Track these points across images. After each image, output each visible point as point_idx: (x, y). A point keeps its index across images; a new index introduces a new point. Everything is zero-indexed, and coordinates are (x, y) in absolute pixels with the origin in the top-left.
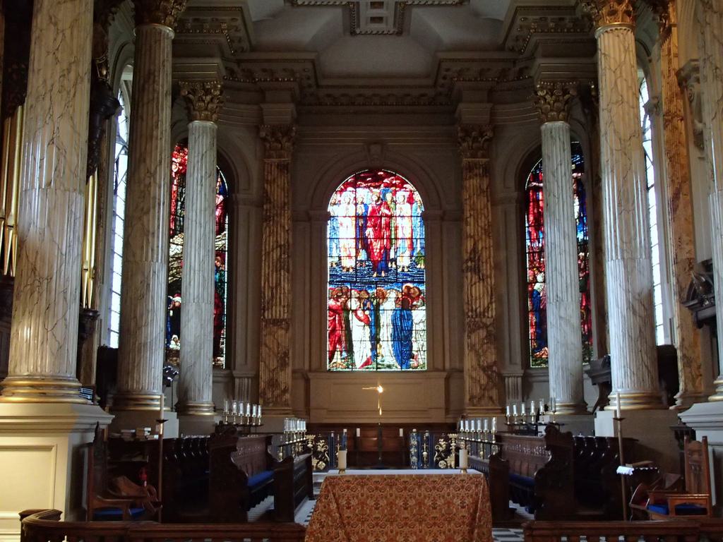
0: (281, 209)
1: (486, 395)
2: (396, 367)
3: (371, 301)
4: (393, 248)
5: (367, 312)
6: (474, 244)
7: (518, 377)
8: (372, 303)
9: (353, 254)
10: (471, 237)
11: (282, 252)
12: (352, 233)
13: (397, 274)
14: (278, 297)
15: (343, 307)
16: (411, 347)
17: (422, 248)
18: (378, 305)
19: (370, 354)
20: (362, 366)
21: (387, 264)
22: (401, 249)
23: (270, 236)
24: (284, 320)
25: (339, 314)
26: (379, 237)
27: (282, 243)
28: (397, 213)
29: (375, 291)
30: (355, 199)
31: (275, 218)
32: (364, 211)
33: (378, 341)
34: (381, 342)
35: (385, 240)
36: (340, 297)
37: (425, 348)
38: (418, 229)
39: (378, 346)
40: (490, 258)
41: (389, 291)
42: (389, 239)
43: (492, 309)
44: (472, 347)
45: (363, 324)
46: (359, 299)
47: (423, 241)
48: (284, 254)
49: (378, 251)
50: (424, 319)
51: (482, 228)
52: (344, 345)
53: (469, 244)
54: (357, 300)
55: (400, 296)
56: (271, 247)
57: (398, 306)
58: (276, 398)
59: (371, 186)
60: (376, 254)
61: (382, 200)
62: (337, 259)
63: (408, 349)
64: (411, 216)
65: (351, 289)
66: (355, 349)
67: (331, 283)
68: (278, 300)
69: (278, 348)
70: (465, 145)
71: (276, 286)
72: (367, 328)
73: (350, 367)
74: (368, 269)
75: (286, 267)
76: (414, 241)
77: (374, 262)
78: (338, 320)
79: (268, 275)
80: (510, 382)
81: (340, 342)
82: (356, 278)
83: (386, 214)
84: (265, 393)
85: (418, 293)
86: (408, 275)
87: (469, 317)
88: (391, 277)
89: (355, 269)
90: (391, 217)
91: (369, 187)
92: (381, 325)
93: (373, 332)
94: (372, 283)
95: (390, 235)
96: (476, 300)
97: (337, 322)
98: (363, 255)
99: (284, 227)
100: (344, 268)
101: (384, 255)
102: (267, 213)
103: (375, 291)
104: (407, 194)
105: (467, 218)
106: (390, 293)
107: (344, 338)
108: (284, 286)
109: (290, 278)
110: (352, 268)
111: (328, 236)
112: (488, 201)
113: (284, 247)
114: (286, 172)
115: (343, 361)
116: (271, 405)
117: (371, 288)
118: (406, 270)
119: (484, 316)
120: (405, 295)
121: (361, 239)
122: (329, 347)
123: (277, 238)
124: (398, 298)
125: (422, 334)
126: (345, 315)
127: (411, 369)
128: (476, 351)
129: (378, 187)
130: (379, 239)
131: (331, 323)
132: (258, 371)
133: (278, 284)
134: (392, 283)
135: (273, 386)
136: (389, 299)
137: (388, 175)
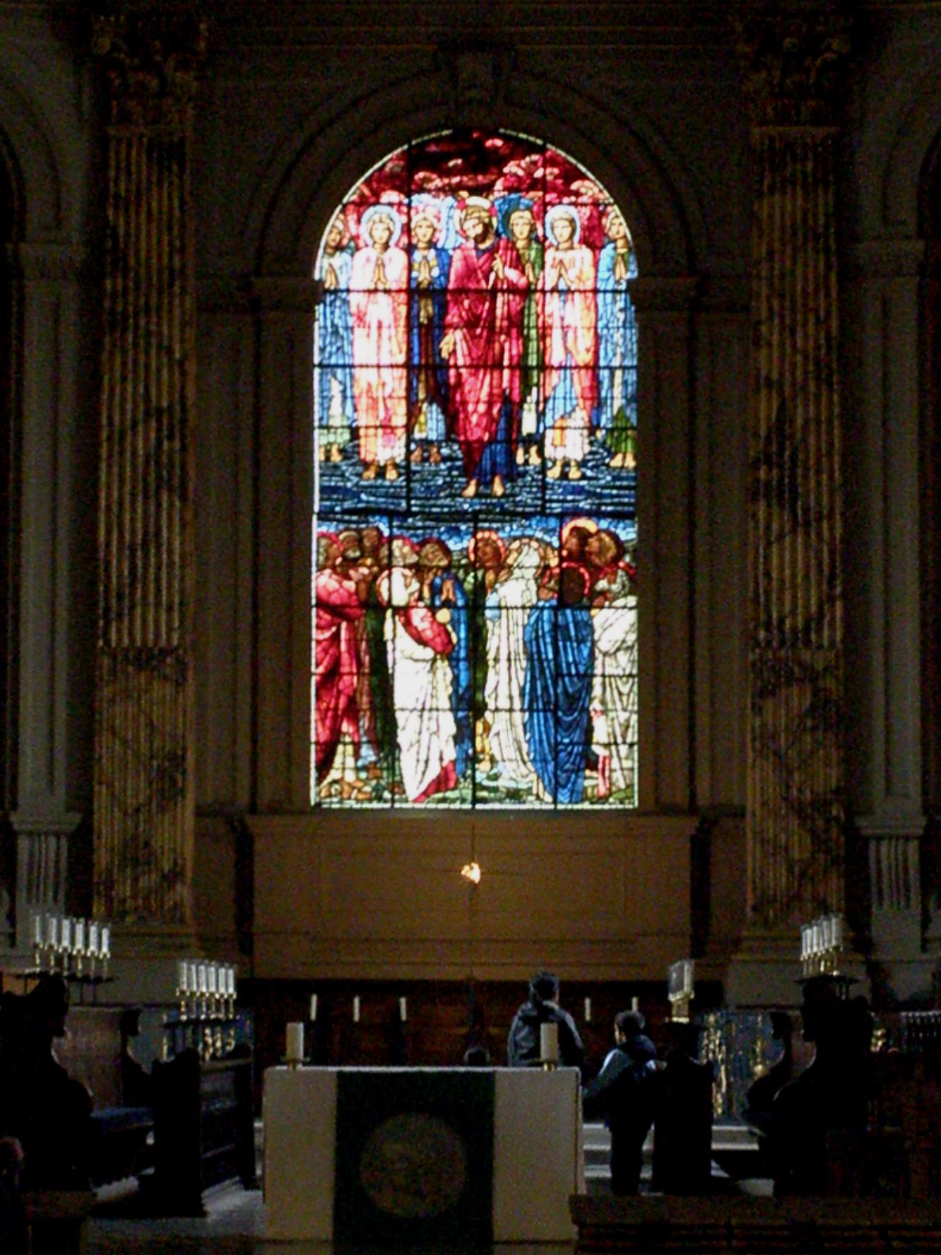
0: (160, 293)
1: (807, 894)
2: (538, 797)
3: (456, 578)
4: (532, 398)
5: (444, 615)
6: (782, 408)
7: (907, 838)
8: (459, 583)
9: (400, 419)
10: (769, 383)
11: (165, 433)
12: (394, 348)
13: (544, 487)
14: (152, 577)
15: (363, 595)
16: (589, 731)
17: (629, 400)
18: (481, 590)
19: (451, 753)
20: (426, 794)
21: (511, 455)
22: (559, 403)
23: (124, 379)
24: (165, 652)
25: (350, 620)
26: (486, 362)
27: (165, 404)
28: (550, 278)
29: (469, 543)
30: (407, 229)
31: (142, 322)
32: (436, 272)
33: (478, 709)
34: (488, 715)
35: (506, 373)
36: (354, 563)
37: (633, 736)
38: (618, 337)
39: (479, 727)
40: (830, 455)
41: (516, 545)
42: (522, 368)
43: (833, 619)
44: (766, 738)
45: (428, 653)
46: (418, 570)
47: (632, 377)
48: (171, 437)
49: (482, 408)
50: (632, 638)
51: (806, 357)
52: (365, 723)
53: (766, 408)
54: (407, 572)
55: (554, 562)
56: (129, 416)
57: (545, 594)
58: (146, 898)
59: (460, 186)
60: (474, 419)
61: (498, 235)
62: (347, 436)
63: (576, 736)
64: (595, 291)
65: (392, 538)
66: (403, 738)
67: (325, 516)
68: (152, 586)
69: (151, 743)
70: (759, 78)
71: (145, 543)
72: (443, 667)
73: (387, 795)
74: (450, 469)
75: (176, 482)
76: (604, 374)
77: (467, 446)
78: (348, 641)
79: (121, 504)
80: (885, 855)
81: (352, 712)
82: (408, 499)
83: (511, 284)
84: (110, 886)
85: (612, 552)
86: (579, 491)
87: (758, 644)
88: (524, 497)
89: (406, 470)
90: (526, 292)
91: (452, 191)
92: (491, 656)
93: (464, 681)
94: (461, 516)
95: (524, 355)
96: (781, 590)
97: (343, 646)
98: (432, 423)
99: (170, 351)
100: (366, 465)
101: (502, 424)
102: (114, 303)
103: (469, 543)
104: (581, 215)
105: (759, 323)
106: (519, 551)
107: (365, 699)
108: (170, 544)
109: (189, 516)
110: (396, 466)
111: (316, 360)
112: (828, 268)
113: (171, 417)
114: (175, 168)
115: (363, 775)
116: (129, 919)
117: (456, 532)
118: (574, 473)
119: (808, 643)
120: (570, 557)
121: (427, 366)
122: (317, 731)
123: (147, 387)
124: (547, 567)
125: (625, 690)
126: (370, 623)
127: (586, 806)
128: (776, 753)
129: (483, 190)
130: (485, 367)
131: (326, 651)
132: (88, 813)
133: (152, 538)
134: (527, 516)
135: (136, 862)
136: (517, 573)
137: (519, 149)
